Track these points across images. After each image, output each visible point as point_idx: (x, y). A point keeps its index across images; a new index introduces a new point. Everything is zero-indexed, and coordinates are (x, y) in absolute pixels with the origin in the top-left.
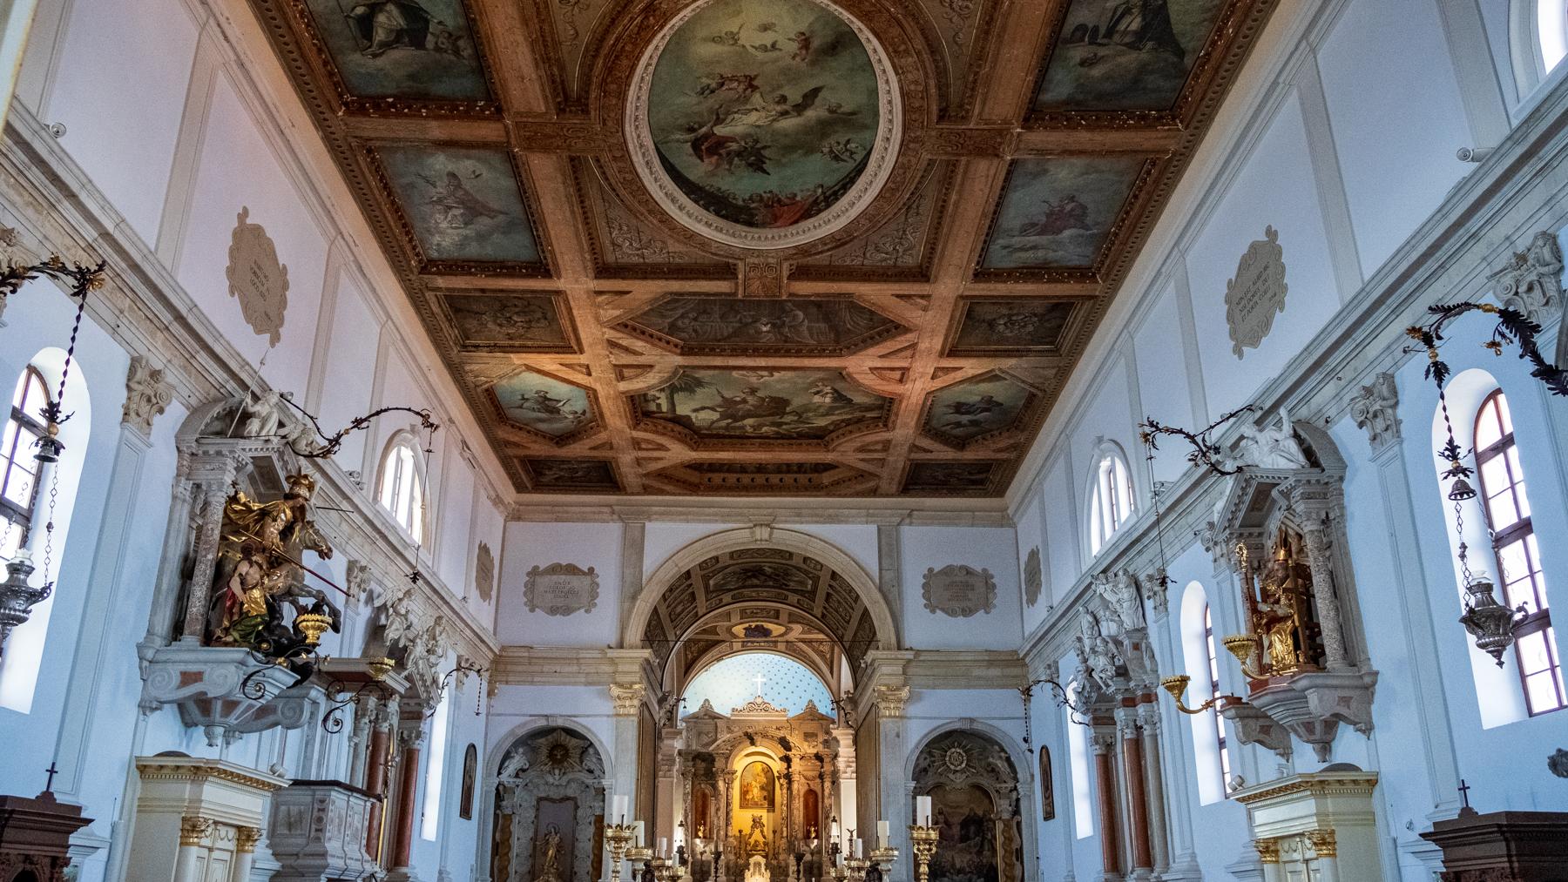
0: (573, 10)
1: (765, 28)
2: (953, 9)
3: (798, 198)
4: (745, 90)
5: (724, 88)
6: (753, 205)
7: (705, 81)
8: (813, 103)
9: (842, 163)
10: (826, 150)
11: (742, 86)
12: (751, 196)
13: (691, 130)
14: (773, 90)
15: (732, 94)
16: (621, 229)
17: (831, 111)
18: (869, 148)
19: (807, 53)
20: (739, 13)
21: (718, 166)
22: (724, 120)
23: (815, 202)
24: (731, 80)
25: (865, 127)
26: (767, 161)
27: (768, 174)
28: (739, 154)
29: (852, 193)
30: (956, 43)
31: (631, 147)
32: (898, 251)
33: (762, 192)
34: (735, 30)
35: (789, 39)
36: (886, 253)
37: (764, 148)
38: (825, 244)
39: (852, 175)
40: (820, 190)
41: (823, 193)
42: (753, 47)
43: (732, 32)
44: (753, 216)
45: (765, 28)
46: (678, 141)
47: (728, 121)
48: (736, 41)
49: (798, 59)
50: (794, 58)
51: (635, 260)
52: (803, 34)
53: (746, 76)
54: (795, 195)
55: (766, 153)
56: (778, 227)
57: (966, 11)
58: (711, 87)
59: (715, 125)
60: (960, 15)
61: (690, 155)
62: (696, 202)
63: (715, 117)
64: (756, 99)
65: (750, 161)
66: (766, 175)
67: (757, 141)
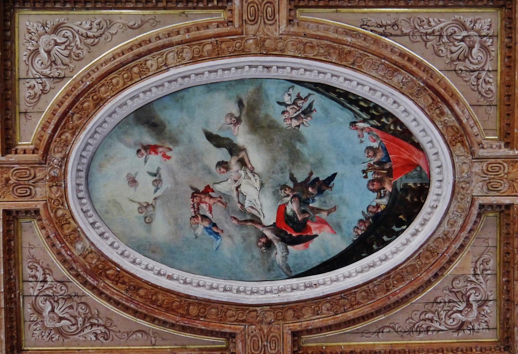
0: (113, 331)
1: (133, 181)
2: (101, 35)
3: (375, 145)
4: (211, 197)
5: (208, 214)
6: (389, 188)
7: (200, 230)
8: (228, 139)
9: (315, 106)
10: (295, 123)
11: (207, 200)
12: (373, 191)
13: (269, 245)
14: (210, 172)
15: (218, 208)
16: (432, 320)
17: (238, 121)
18: (290, 84)
19: (161, 147)
20: (116, 203)
21: (323, 222)
22: (253, 215)
23: (383, 128)
24: (198, 209)
25: (259, 90)
26: (314, 177)
27: (335, 175)
28: (303, 202)
29: (363, 92)
30: (139, 27)
31: (277, 301)
32: (464, 37)
33: (366, 181)
34: (137, 206)
35: (146, 162)
36: (471, 48)
37: (293, 178)
38: (442, 113)
39: (334, 95)
40: (361, 125)
41: (364, 121)
42: (155, 191)
43: (139, 208)
44: (406, 189)
45: (133, 181)
46: (285, 258)
47: (254, 212)
48: (148, 205)
49: (168, 154)
50: (169, 158)
51: (490, 309)
52: (139, 151)
53: (193, 196)
54: (369, 148)
55: (301, 177)
56: (427, 162)
57: (103, 23)
58: (208, 226)
59: (261, 223)
60: (108, 28)
61: (307, 247)
62: (384, 244)
63: (249, 224)
64: (222, 188)
65: (315, 193)
66: (336, 178)
67: (284, 187)
